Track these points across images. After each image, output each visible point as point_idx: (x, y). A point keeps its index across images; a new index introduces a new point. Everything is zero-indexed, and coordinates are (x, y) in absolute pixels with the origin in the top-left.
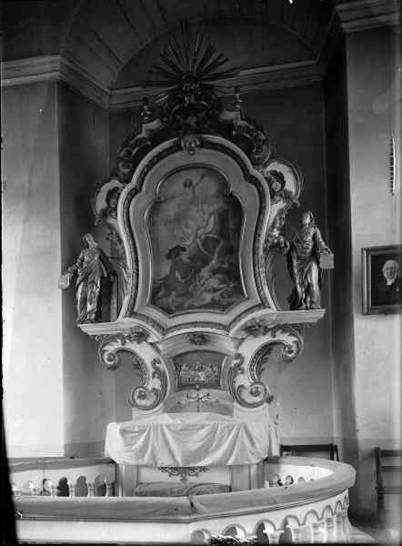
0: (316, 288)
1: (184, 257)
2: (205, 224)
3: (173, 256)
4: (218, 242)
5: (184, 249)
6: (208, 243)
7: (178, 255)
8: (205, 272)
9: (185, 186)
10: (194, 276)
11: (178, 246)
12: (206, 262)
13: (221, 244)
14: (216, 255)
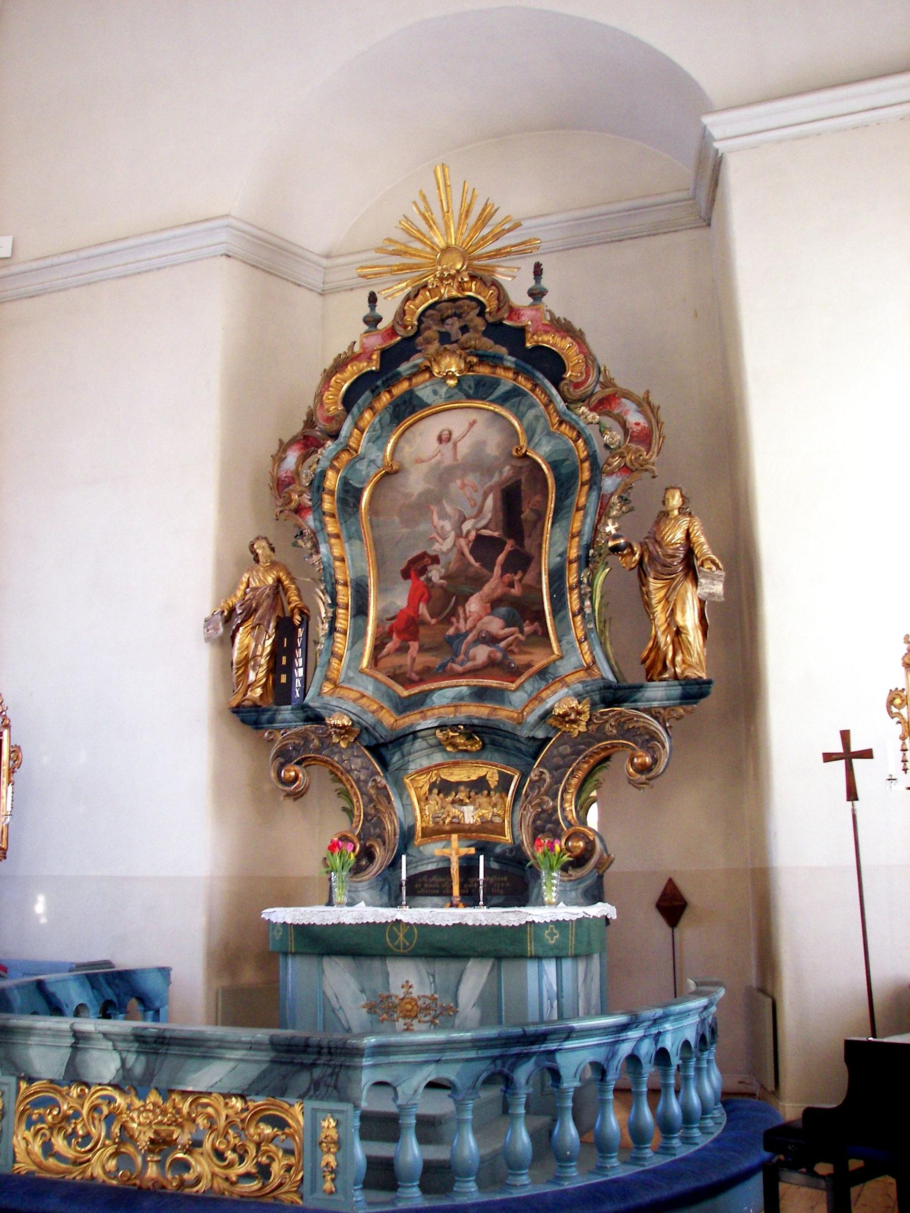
0: (694, 636)
1: (435, 574)
3: (413, 574)
5: (435, 560)
6: (483, 546)
7: (423, 571)
8: (474, 605)
9: (440, 439)
10: (454, 613)
11: (424, 555)
12: (478, 582)
13: (509, 546)
14: (497, 570)
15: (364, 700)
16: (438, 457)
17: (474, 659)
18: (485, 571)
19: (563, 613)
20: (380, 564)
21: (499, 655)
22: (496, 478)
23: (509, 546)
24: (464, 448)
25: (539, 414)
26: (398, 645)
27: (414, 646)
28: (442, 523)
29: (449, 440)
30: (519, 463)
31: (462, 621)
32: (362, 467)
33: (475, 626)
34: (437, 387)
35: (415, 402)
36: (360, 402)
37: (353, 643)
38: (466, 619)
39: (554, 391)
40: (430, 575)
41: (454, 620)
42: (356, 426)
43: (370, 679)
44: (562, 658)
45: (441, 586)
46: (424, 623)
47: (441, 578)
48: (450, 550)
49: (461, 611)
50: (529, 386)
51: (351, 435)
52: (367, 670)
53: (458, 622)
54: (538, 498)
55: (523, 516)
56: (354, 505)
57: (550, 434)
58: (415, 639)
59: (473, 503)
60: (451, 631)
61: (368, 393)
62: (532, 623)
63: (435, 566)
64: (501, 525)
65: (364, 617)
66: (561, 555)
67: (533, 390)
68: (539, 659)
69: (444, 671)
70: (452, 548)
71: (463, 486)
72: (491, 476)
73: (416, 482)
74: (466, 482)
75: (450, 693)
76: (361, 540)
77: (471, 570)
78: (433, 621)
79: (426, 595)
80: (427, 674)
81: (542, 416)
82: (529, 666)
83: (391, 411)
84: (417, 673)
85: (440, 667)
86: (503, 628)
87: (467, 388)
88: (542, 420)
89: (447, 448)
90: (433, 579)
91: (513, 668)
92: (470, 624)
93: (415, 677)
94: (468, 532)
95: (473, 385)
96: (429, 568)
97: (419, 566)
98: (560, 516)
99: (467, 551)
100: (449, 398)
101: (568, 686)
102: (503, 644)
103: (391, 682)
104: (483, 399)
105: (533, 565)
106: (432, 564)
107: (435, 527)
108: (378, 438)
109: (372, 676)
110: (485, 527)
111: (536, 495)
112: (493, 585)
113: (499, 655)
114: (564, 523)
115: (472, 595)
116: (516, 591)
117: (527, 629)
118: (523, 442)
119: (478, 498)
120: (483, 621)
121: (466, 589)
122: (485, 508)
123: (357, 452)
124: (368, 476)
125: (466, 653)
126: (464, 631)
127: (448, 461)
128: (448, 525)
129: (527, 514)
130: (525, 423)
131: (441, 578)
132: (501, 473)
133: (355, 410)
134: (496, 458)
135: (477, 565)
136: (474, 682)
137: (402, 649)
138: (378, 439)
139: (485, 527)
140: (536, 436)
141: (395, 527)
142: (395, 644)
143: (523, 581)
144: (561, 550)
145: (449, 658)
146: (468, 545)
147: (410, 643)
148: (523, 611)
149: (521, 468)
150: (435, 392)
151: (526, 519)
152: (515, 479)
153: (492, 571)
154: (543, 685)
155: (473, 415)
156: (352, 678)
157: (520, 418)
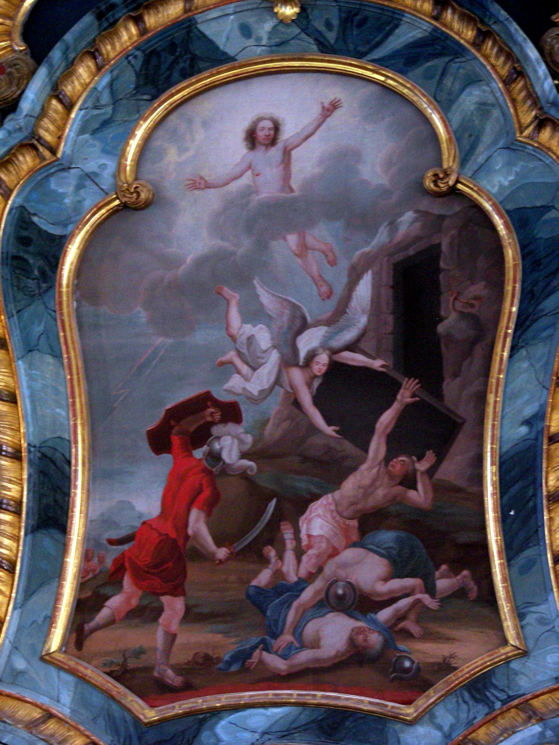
1: (229, 444)
2: (330, 306)
3: (176, 440)
4: (380, 388)
5: (231, 413)
6: (346, 390)
7: (202, 436)
8: (319, 522)
9: (251, 138)
10: (272, 536)
11: (205, 400)
12: (331, 470)
13: (405, 395)
14: (377, 446)
15: (51, 726)
16: (246, 180)
17: (315, 644)
18: (348, 447)
19: (529, 553)
20: (99, 414)
21: (375, 639)
22: (382, 237)
23: (405, 395)
24: (307, 162)
25: (491, 99)
26: (134, 602)
27: (174, 607)
28: (248, 329)
29: (273, 141)
30: (437, 208)
31: (290, 556)
32: (64, 186)
33: (320, 570)
34: (251, 20)
35: (197, 49)
36: (68, 37)
37: (28, 593)
38: (299, 553)
39: (532, 52)
40: (217, 446)
41: (272, 553)
42: (56, 92)
43: (69, 678)
44: (525, 654)
45: (244, 475)
46: (200, 556)
47: (244, 455)
48: (265, 394)
49: (288, 535)
50: (470, 34)
51: (43, 112)
52: (61, 657)
53: (281, 556)
54: (478, 289)
55: (441, 328)
56: (43, 273)
57: (513, 147)
58: (177, 590)
59: (324, 289)
60: (263, 578)
61: (88, 19)
62: (455, 571)
63: (231, 427)
64: (389, 342)
65: (58, 536)
66: (528, 422)
67: (477, 44)
68: (471, 655)
69: (245, 670)
70: (272, 389)
71: (304, 249)
72: (372, 231)
73: (190, 232)
74: (310, 240)
75: (260, 719)
76: (58, 356)
77: (317, 440)
78: (222, 553)
79: (207, 493)
80: (202, 672)
81: (496, 104)
82: (446, 667)
83: (138, 64)
84: (178, 670)
85: (235, 658)
86: (386, 580)
87: (322, 28)
88: (496, 113)
89: (268, 160)
90: (225, 456)
91: (408, 670)
92: (308, 563)
93: (172, 677)
94: (312, 356)
95: (335, 22)
96: (216, 430)
97: (191, 424)
98: (529, 334)
99: (306, 399)
100: (279, 46)
101: (541, 720)
102: (384, 615)
103: (117, 688)
104: (359, 55)
105: (462, 441)
106: (225, 420)
107: (233, 338)
108: (106, 123)
109: (72, 672)
110: (352, 347)
111: (472, 280)
112: (367, 478)
113: (375, 639)
114: (540, 350)
115: (315, 497)
116: (419, 496)
117: (443, 584)
118: (449, 160)
119: (338, 279)
120: (338, 559)
121: (302, 484)
122: (354, 303)
123: (53, 151)
124: (78, 207)
125: (298, 630)
126: (293, 578)
127: (269, 186)
128: (263, 337)
129: (450, 323)
130: (456, 119)
131: (244, 455)
132: (393, 226)
133: (56, 54)
134: (385, 192)
135: (330, 430)
136: (319, 696)
137: (145, 613)
138: (106, 127)
139: (352, 347)
140: (481, 148)
141: (137, 328)
142: (128, 599)
143: (438, 475)
144: (529, 411)
145: (254, 640)
146: (309, 385)
147: (165, 599)
148: (438, 541)
149: (442, 218)
150: (246, 31)
151: (449, 336)
152: (422, 245)
153: (366, 451)
154: (480, 711)
155: (332, 91)
156: (22, 673)
157: (445, 106)
